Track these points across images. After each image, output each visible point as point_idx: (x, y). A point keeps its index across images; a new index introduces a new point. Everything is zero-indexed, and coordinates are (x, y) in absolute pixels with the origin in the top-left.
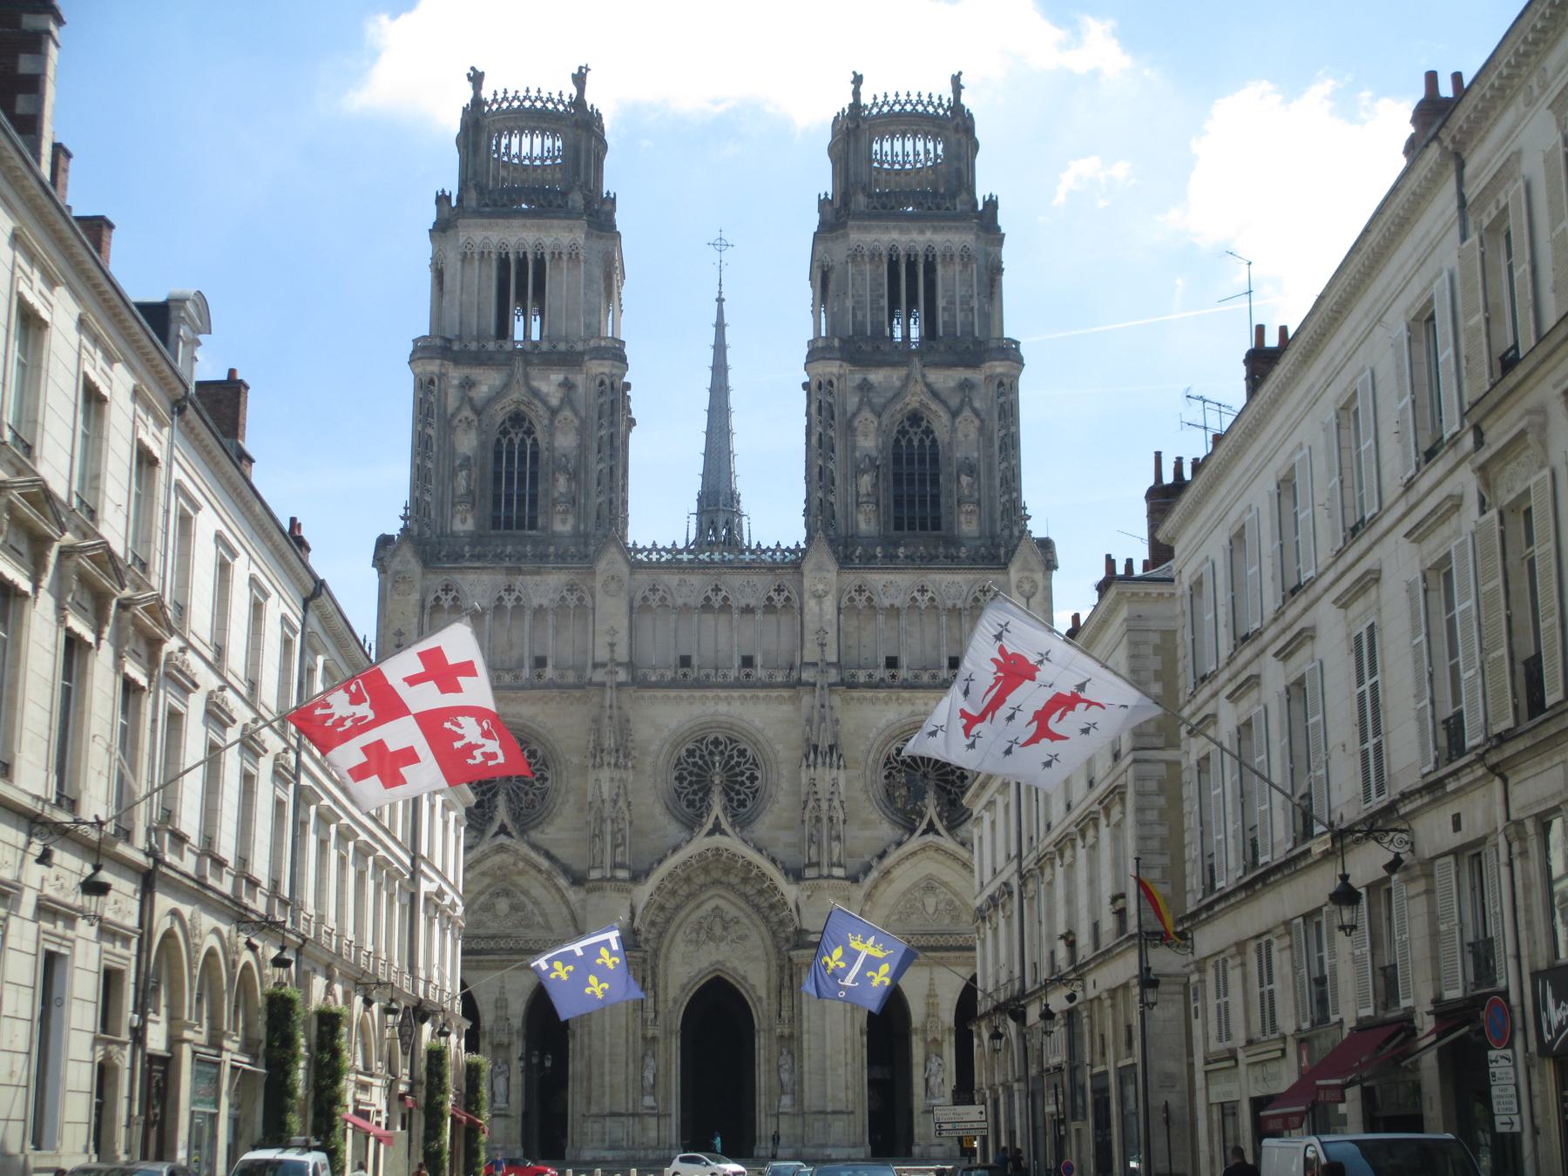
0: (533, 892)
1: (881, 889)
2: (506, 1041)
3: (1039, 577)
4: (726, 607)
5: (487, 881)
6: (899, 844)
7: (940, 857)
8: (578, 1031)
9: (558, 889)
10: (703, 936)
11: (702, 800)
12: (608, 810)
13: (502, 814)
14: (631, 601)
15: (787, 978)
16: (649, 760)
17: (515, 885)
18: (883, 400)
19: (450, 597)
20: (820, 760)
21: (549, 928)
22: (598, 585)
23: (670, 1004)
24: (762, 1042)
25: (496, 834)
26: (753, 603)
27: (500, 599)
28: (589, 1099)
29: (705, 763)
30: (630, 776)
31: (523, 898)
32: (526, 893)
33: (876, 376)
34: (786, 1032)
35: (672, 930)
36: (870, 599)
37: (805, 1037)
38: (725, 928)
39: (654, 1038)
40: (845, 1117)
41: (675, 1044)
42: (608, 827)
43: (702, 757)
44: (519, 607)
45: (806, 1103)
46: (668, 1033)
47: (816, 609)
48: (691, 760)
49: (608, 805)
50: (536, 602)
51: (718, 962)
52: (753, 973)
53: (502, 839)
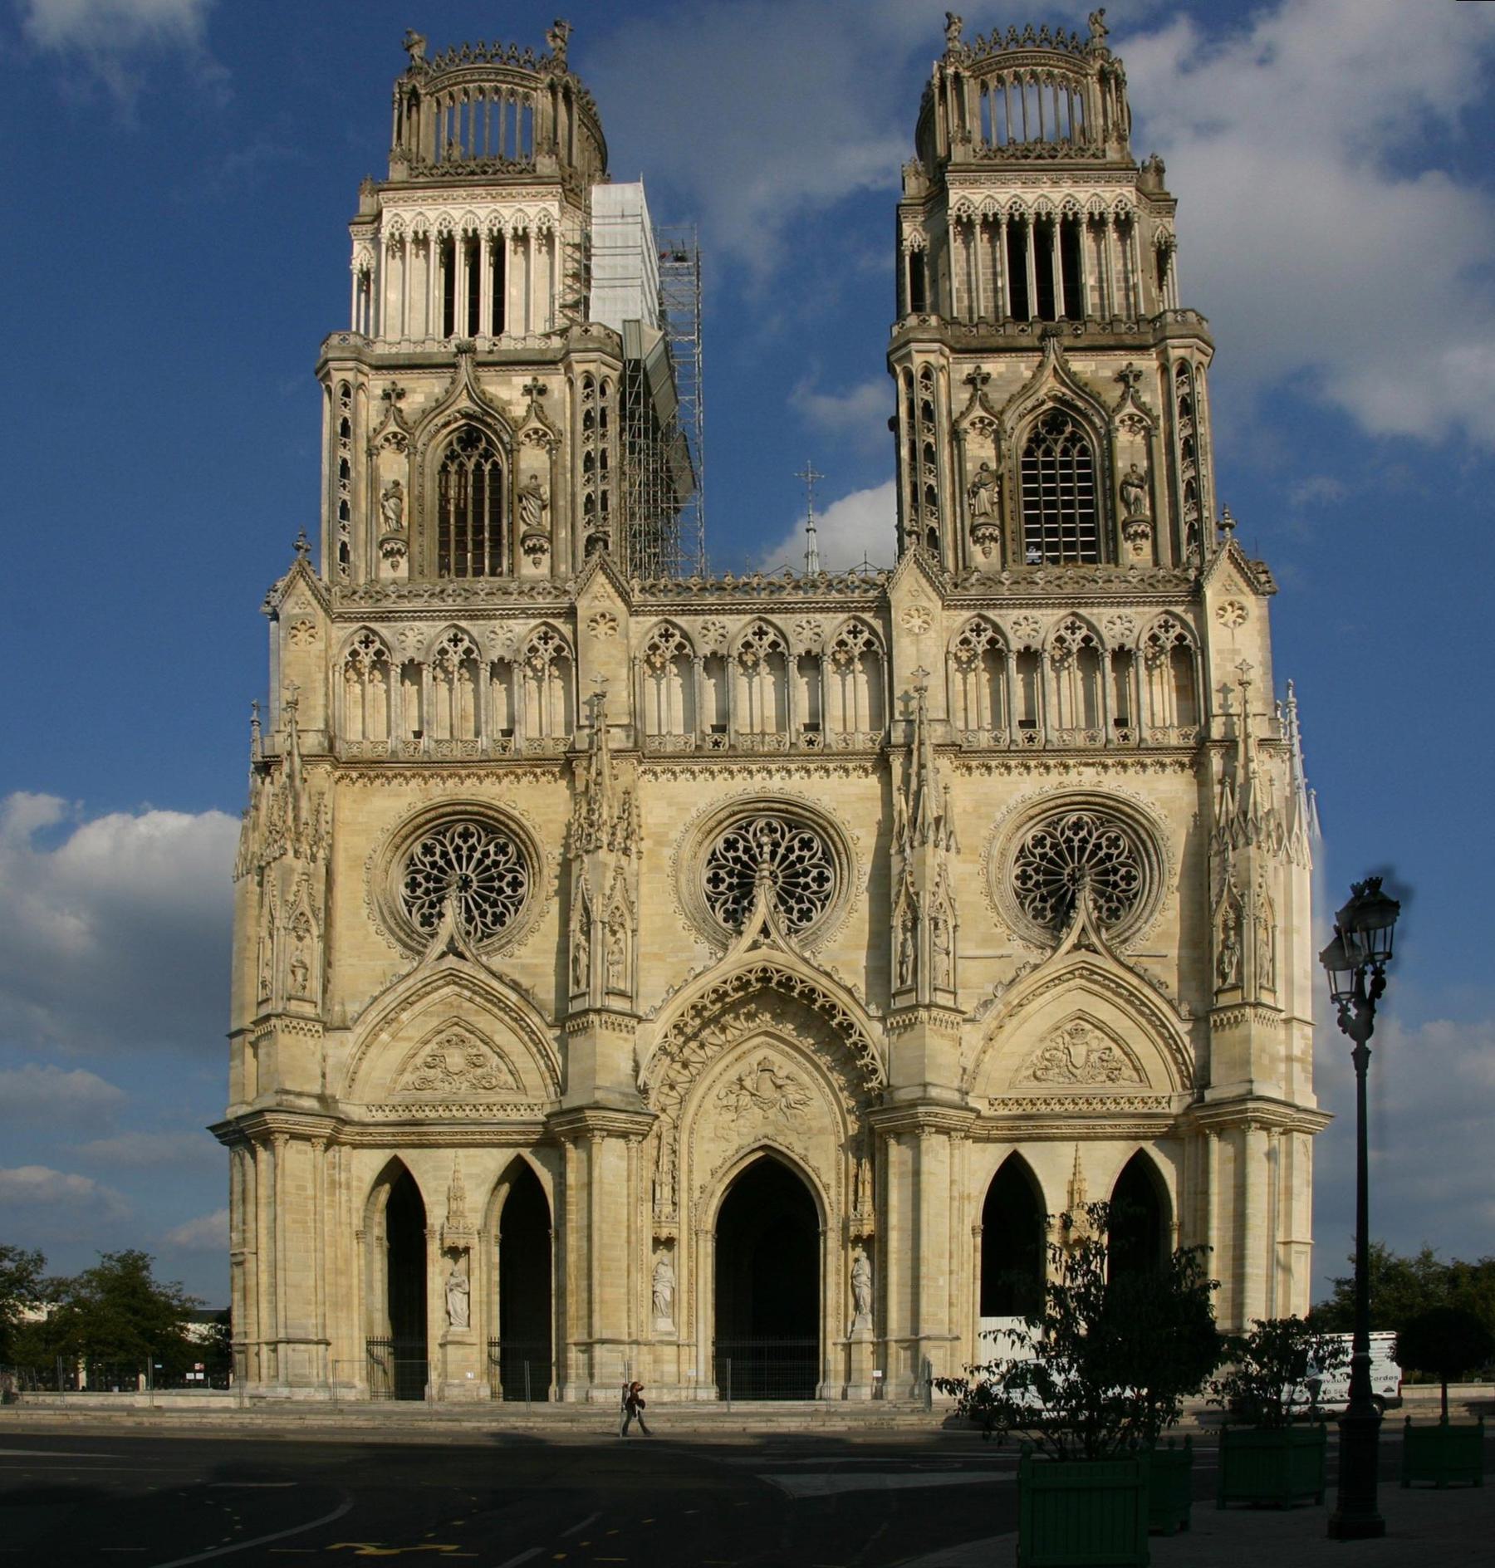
0: (497, 1038)
1: (1008, 1029)
5: (434, 1023)
6: (1036, 967)
10: (746, 1099)
18: (1007, 396)
21: (521, 1088)
23: (697, 1194)
24: (832, 1242)
25: (443, 955)
31: (484, 1049)
33: (993, 366)
47: (912, 650)
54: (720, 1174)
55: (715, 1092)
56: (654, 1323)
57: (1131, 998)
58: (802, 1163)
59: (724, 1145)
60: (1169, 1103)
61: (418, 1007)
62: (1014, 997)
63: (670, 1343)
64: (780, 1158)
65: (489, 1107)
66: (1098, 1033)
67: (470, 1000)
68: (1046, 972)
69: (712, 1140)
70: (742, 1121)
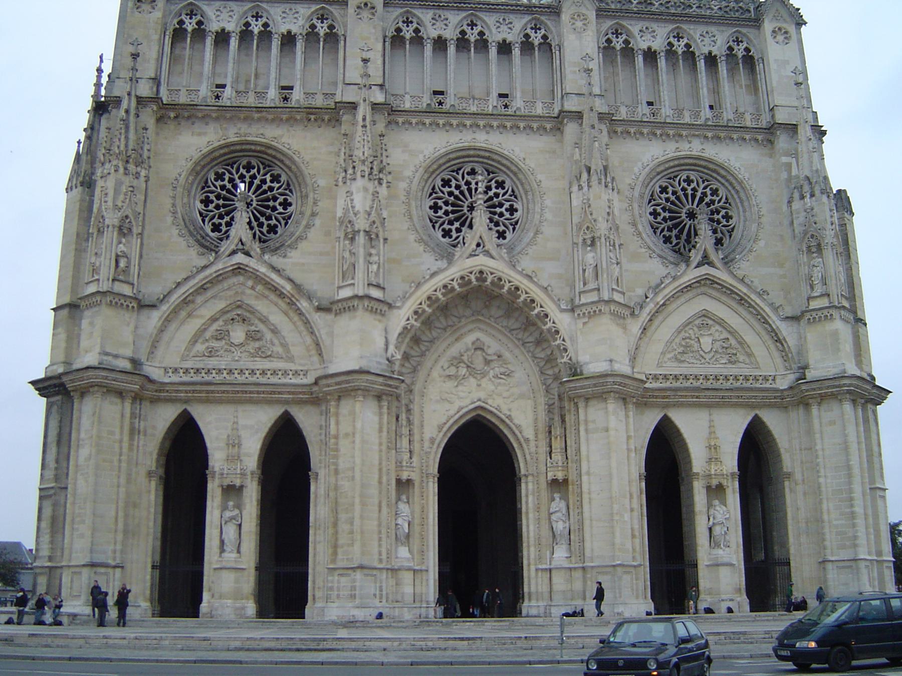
1: (656, 322)
2: (238, 483)
3: (792, 29)
4: (483, 44)
5: (221, 305)
7: (714, 293)
8: (322, 473)
9: (301, 314)
10: (463, 371)
11: (458, 230)
12: (361, 224)
13: (240, 230)
14: (384, 30)
15: (557, 418)
16: (403, 185)
17: (253, 311)
19: (194, 21)
20: (594, 178)
22: (351, 10)
23: (427, 444)
26: (510, 38)
27: (247, 24)
28: (335, 547)
29: (462, 193)
30: (383, 191)
31: (261, 327)
32: (264, 320)
34: (560, 476)
35: (428, 363)
36: (626, 42)
37: (585, 478)
38: (487, 362)
39: (409, 482)
40: (632, 570)
41: (433, 488)
42: (361, 239)
43: (458, 187)
44: (266, 34)
45: (588, 553)
46: (425, 475)
48: (447, 189)
49: (362, 215)
50: (284, 29)
51: (479, 400)
52: (520, 412)
53: (240, 258)
54: (445, 429)
55: (441, 363)
56: (396, 551)
57: (742, 300)
58: (507, 420)
59: (447, 406)
60: (774, 380)
61: (209, 294)
62: (660, 299)
63: (409, 569)
64: (489, 417)
65: (264, 373)
66: (717, 327)
67: (253, 288)
68: (682, 281)
69: (437, 401)
70: (460, 388)
